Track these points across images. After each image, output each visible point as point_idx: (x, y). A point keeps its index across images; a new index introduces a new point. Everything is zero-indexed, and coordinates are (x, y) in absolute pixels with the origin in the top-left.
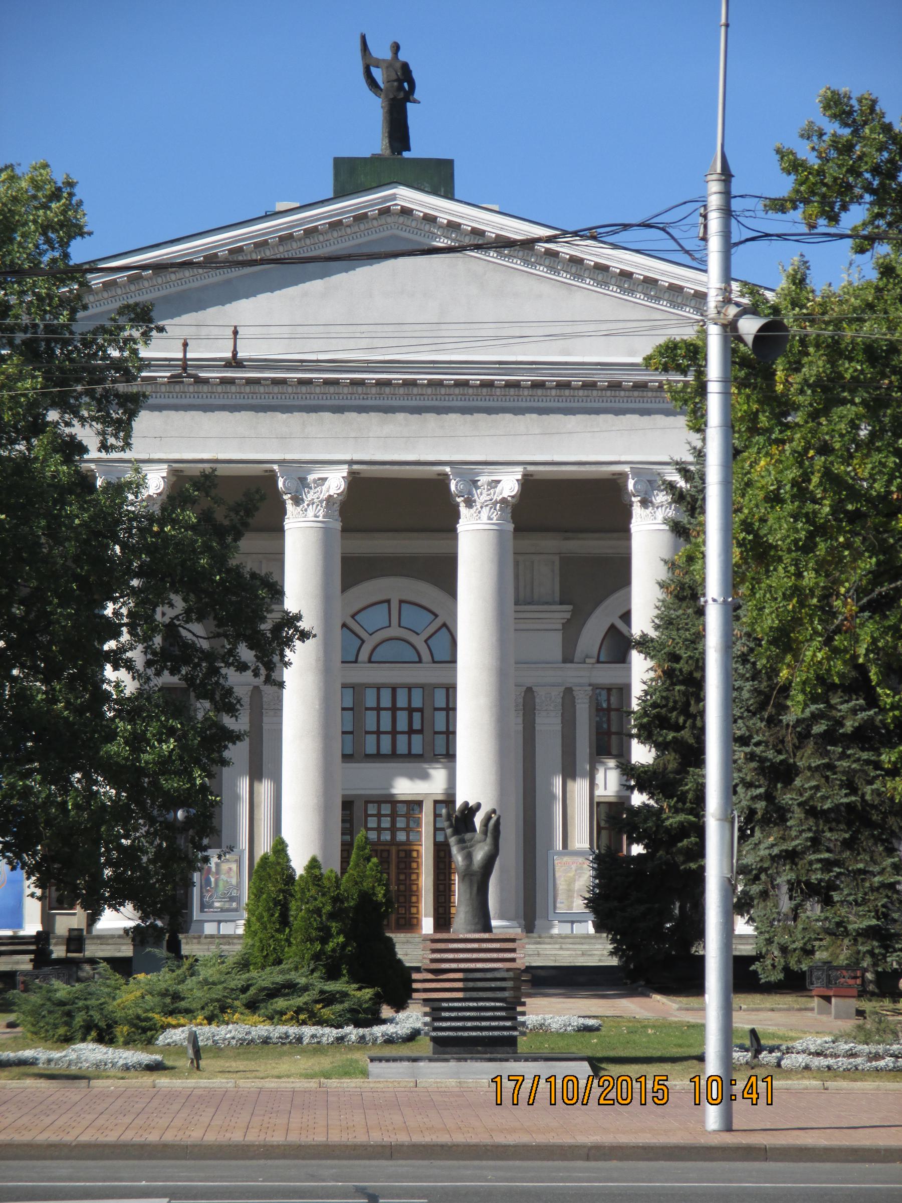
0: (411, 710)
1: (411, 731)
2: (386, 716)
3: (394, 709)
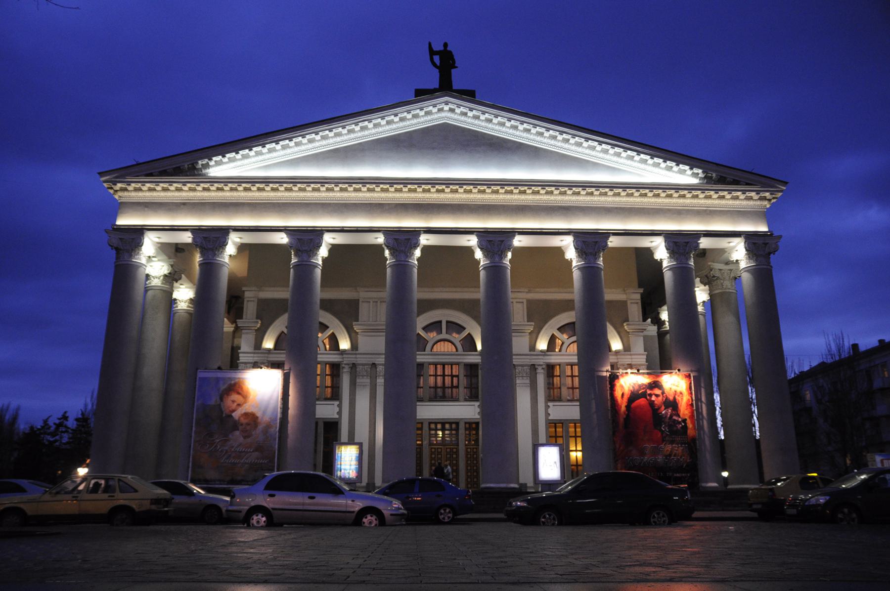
0: (452, 376)
1: (452, 387)
2: (439, 379)
3: (444, 376)
